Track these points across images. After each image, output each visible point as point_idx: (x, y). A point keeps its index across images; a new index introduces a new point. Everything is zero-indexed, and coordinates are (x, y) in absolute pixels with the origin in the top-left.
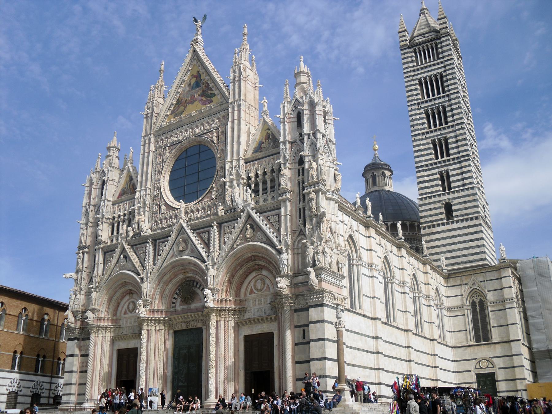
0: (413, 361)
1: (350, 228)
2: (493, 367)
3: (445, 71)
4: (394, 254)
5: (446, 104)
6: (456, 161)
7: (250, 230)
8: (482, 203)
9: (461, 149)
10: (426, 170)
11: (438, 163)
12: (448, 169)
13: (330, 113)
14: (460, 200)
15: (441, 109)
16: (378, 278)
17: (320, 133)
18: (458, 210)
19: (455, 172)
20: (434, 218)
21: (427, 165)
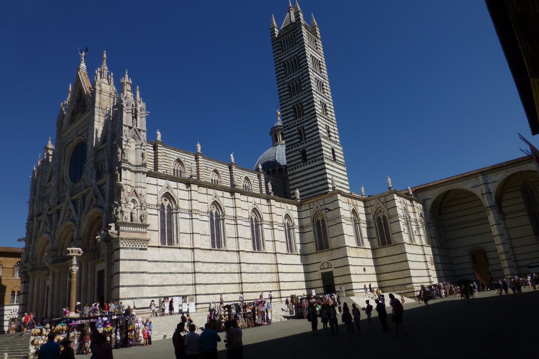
0: (245, 272)
1: (167, 188)
2: (331, 267)
3: (299, 53)
4: (225, 197)
5: (301, 77)
6: (308, 119)
7: (95, 200)
8: (329, 147)
9: (310, 109)
10: (289, 129)
11: (296, 122)
12: (303, 126)
13: (144, 109)
14: (311, 147)
15: (298, 82)
16: (198, 219)
17: (125, 126)
18: (310, 155)
19: (307, 127)
20: (295, 162)
21: (290, 125)
